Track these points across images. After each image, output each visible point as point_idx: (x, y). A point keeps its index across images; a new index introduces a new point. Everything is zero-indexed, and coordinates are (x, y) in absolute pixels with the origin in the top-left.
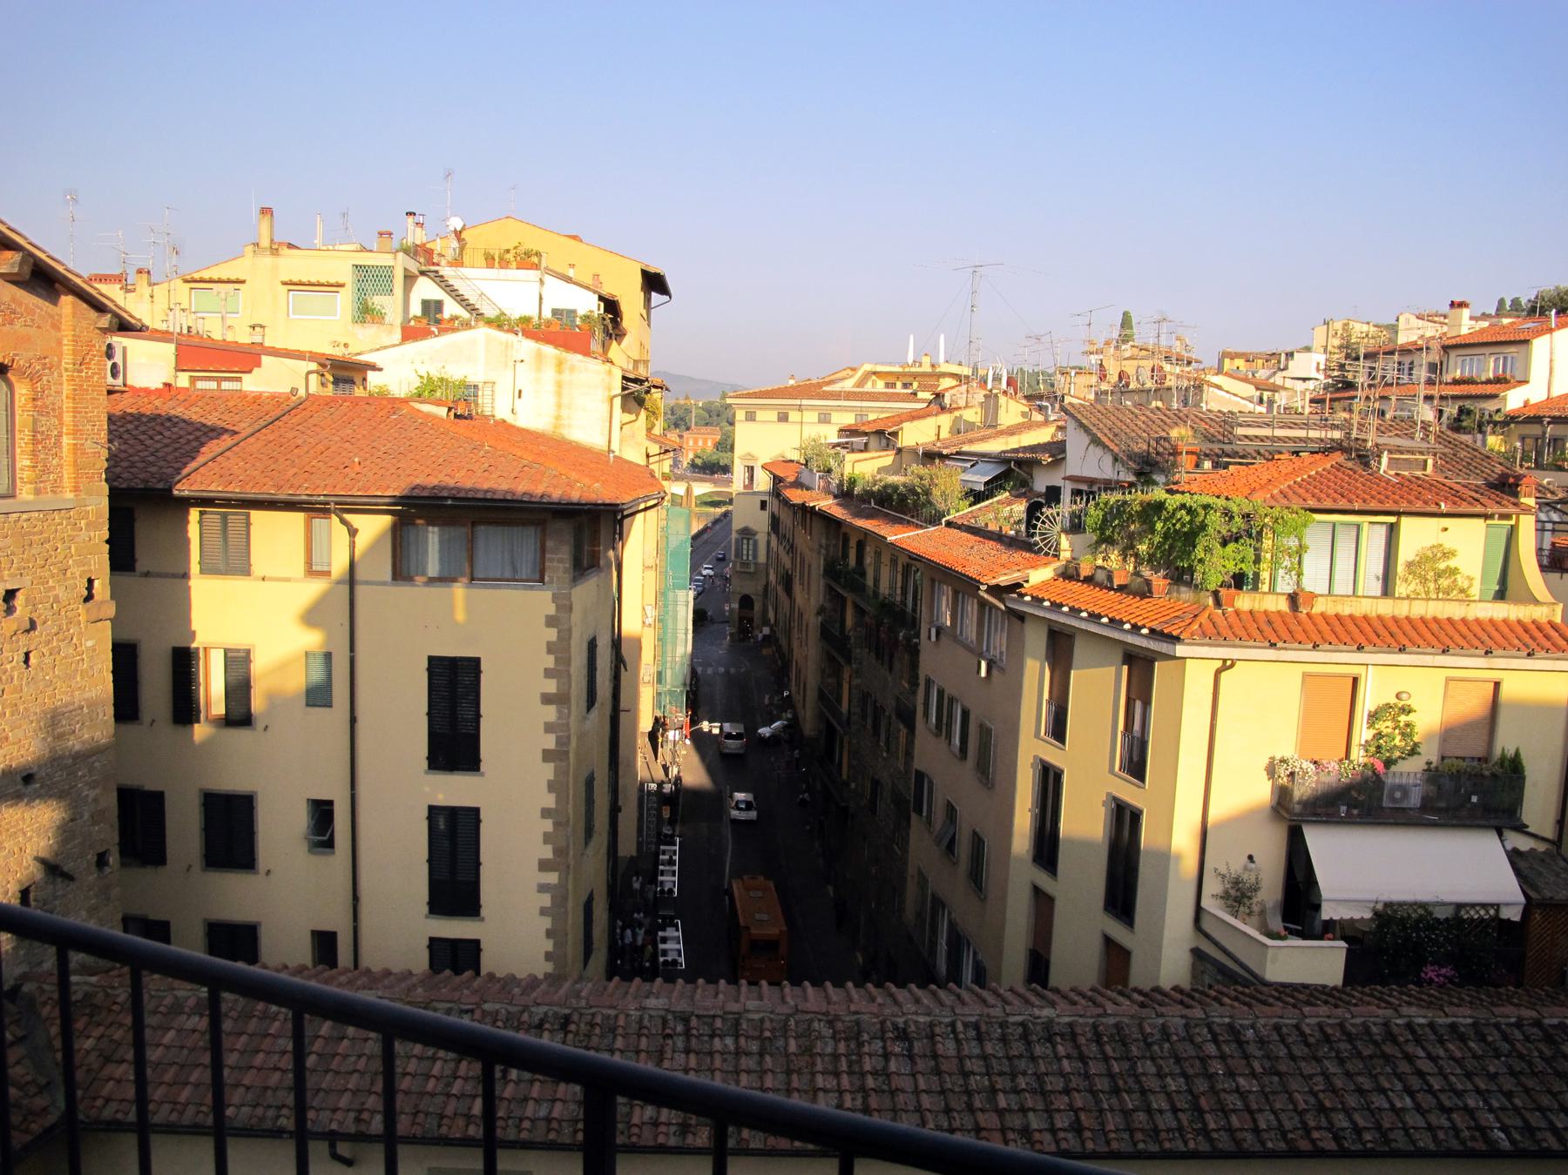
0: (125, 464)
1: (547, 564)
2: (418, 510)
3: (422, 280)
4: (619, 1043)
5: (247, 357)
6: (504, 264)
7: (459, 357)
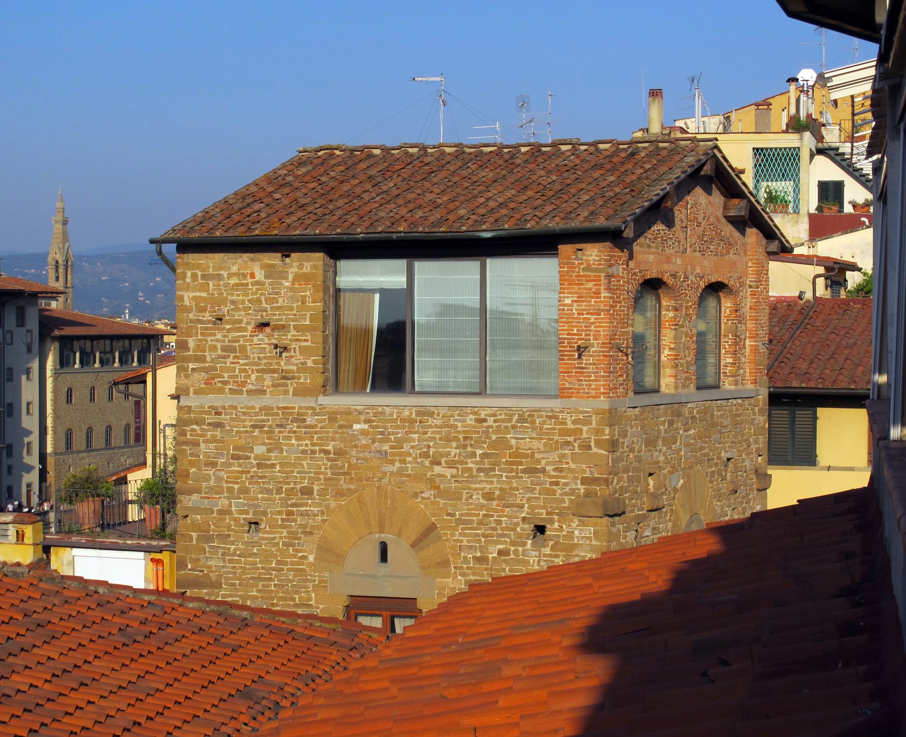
3: (820, 159)
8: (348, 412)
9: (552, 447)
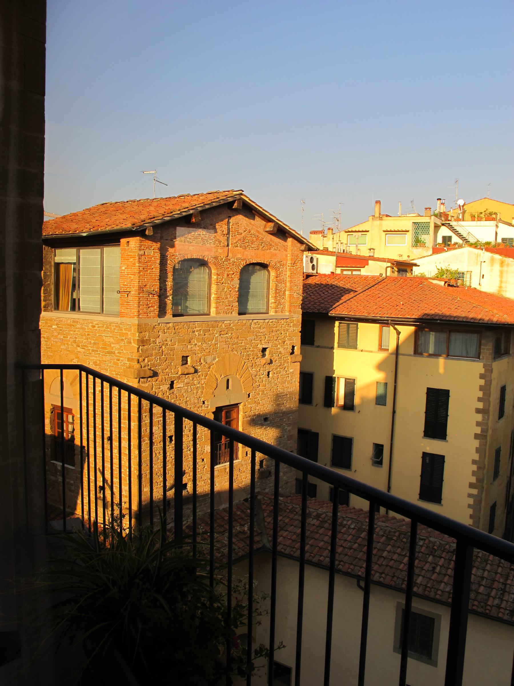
0: (312, 303)
1: (482, 351)
2: (426, 324)
3: (443, 228)
4: (488, 567)
5: (363, 261)
6: (480, 219)
7: (456, 260)
8: (51, 320)
9: (118, 342)
